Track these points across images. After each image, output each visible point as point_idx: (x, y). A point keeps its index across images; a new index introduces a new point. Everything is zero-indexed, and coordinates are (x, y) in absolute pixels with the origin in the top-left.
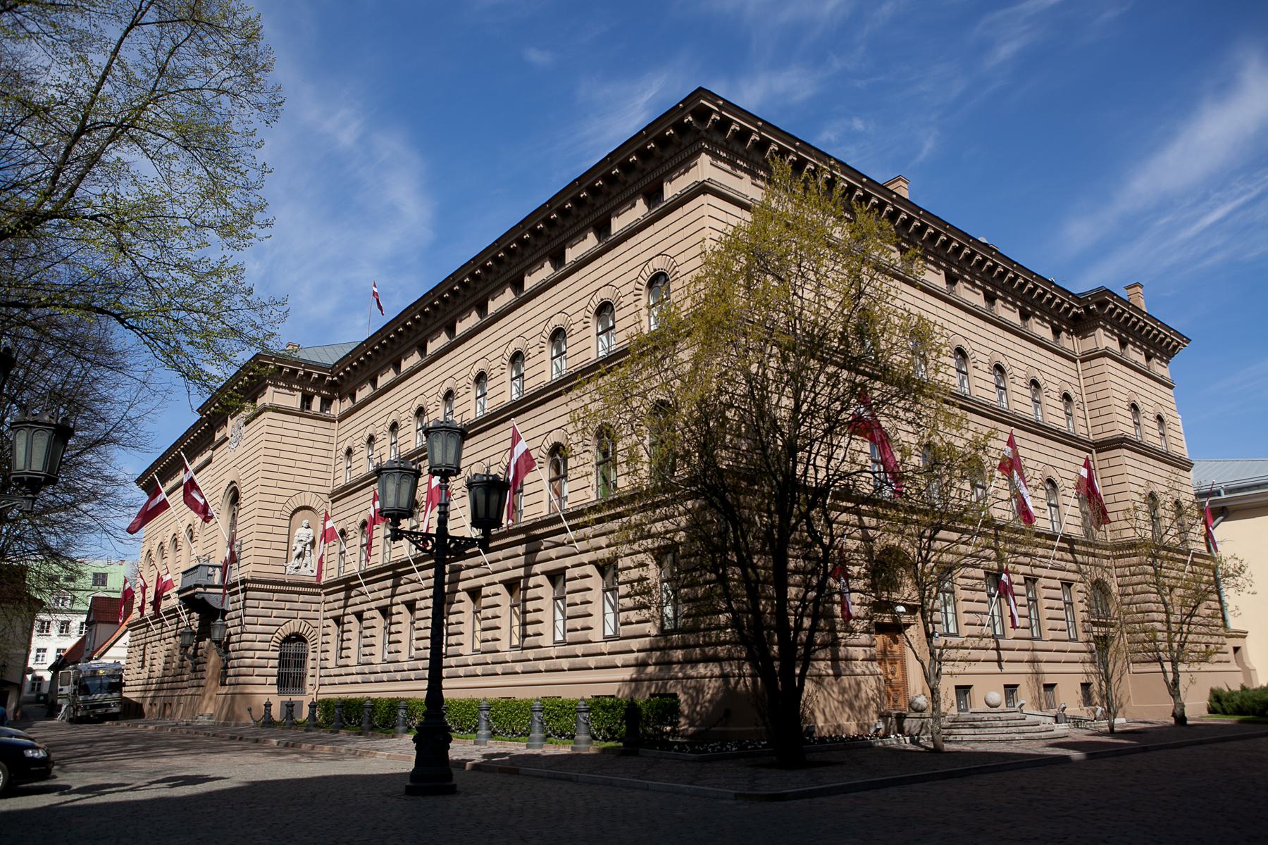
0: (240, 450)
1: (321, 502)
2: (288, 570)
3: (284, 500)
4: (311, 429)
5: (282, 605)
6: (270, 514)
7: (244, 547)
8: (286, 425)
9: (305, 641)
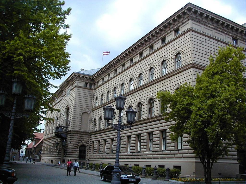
0: (69, 97)
4: (87, 92)
6: (77, 114)
7: (70, 122)
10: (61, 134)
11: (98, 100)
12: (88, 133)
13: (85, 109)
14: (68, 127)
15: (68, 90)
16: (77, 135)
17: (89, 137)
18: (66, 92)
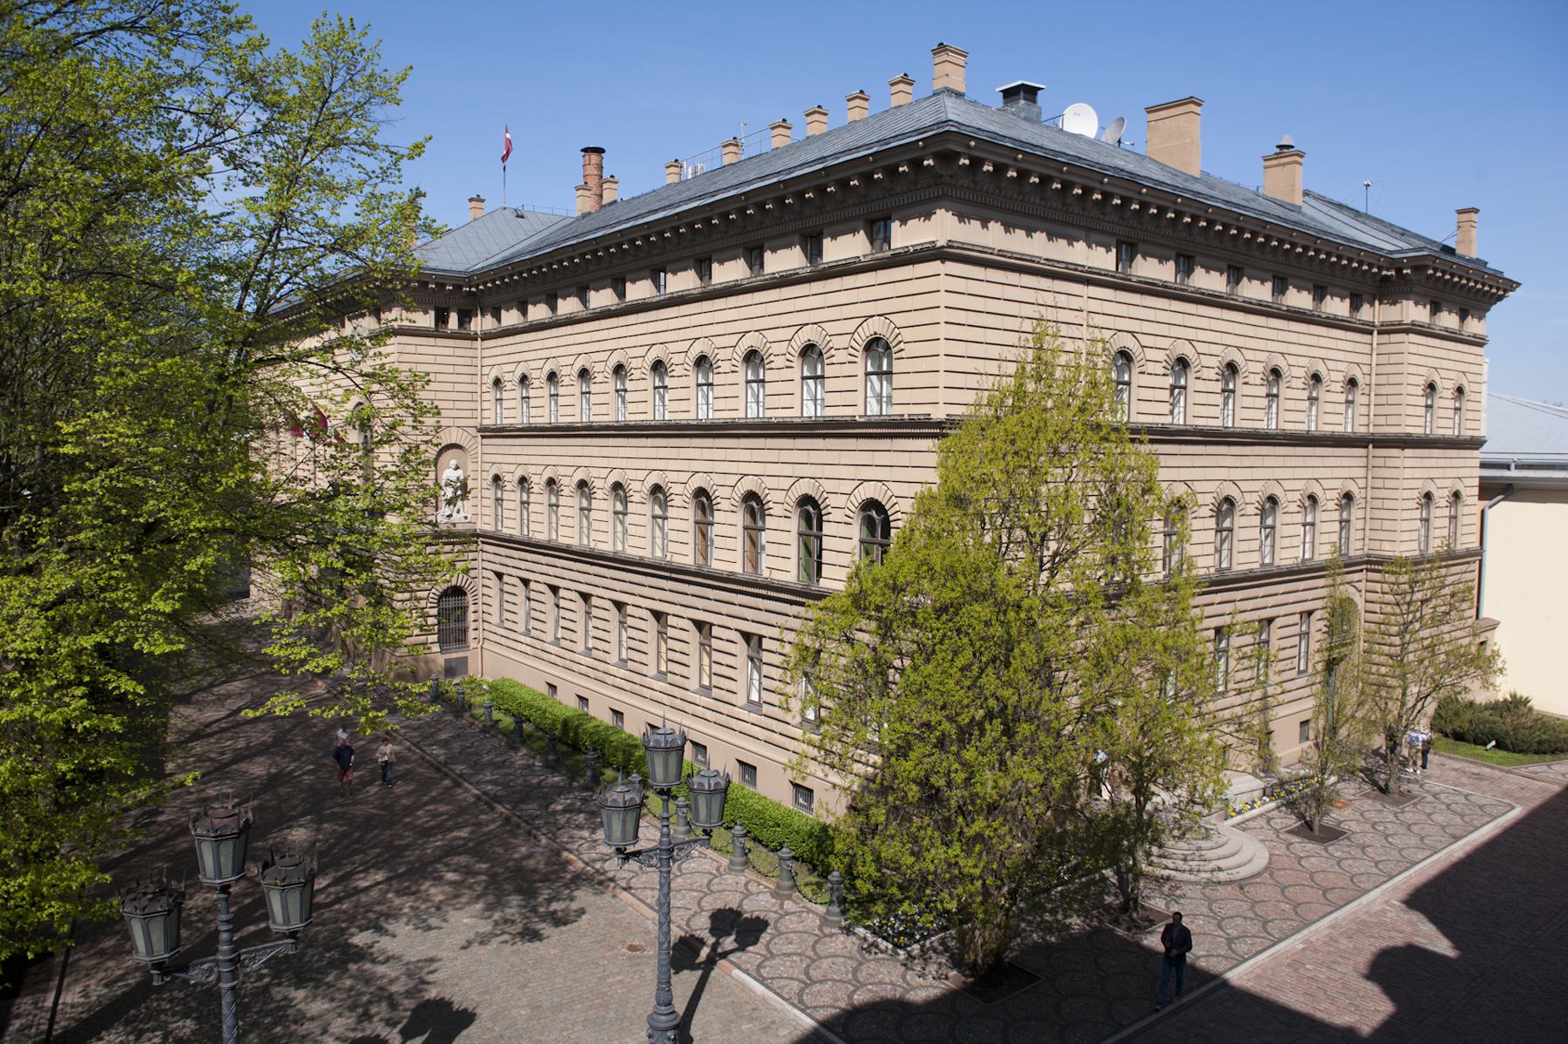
4: (449, 351)
8: (421, 350)
9: (465, 594)
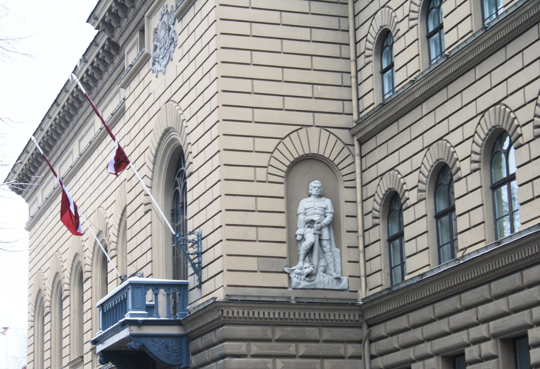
0: (173, 69)
1: (340, 145)
2: (295, 280)
3: (270, 145)
5: (292, 348)
6: (248, 174)
7: (206, 243)
10: (149, 343)
11: (397, 47)
12: (352, 305)
13: (304, 129)
14: (192, 281)
15: (155, 22)
16: (268, 332)
17: (360, 342)
18: (142, 45)
